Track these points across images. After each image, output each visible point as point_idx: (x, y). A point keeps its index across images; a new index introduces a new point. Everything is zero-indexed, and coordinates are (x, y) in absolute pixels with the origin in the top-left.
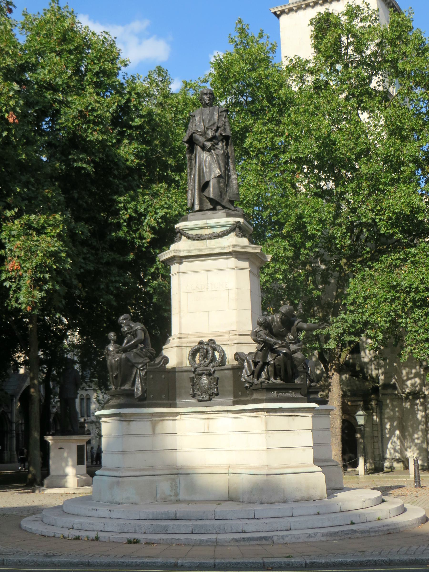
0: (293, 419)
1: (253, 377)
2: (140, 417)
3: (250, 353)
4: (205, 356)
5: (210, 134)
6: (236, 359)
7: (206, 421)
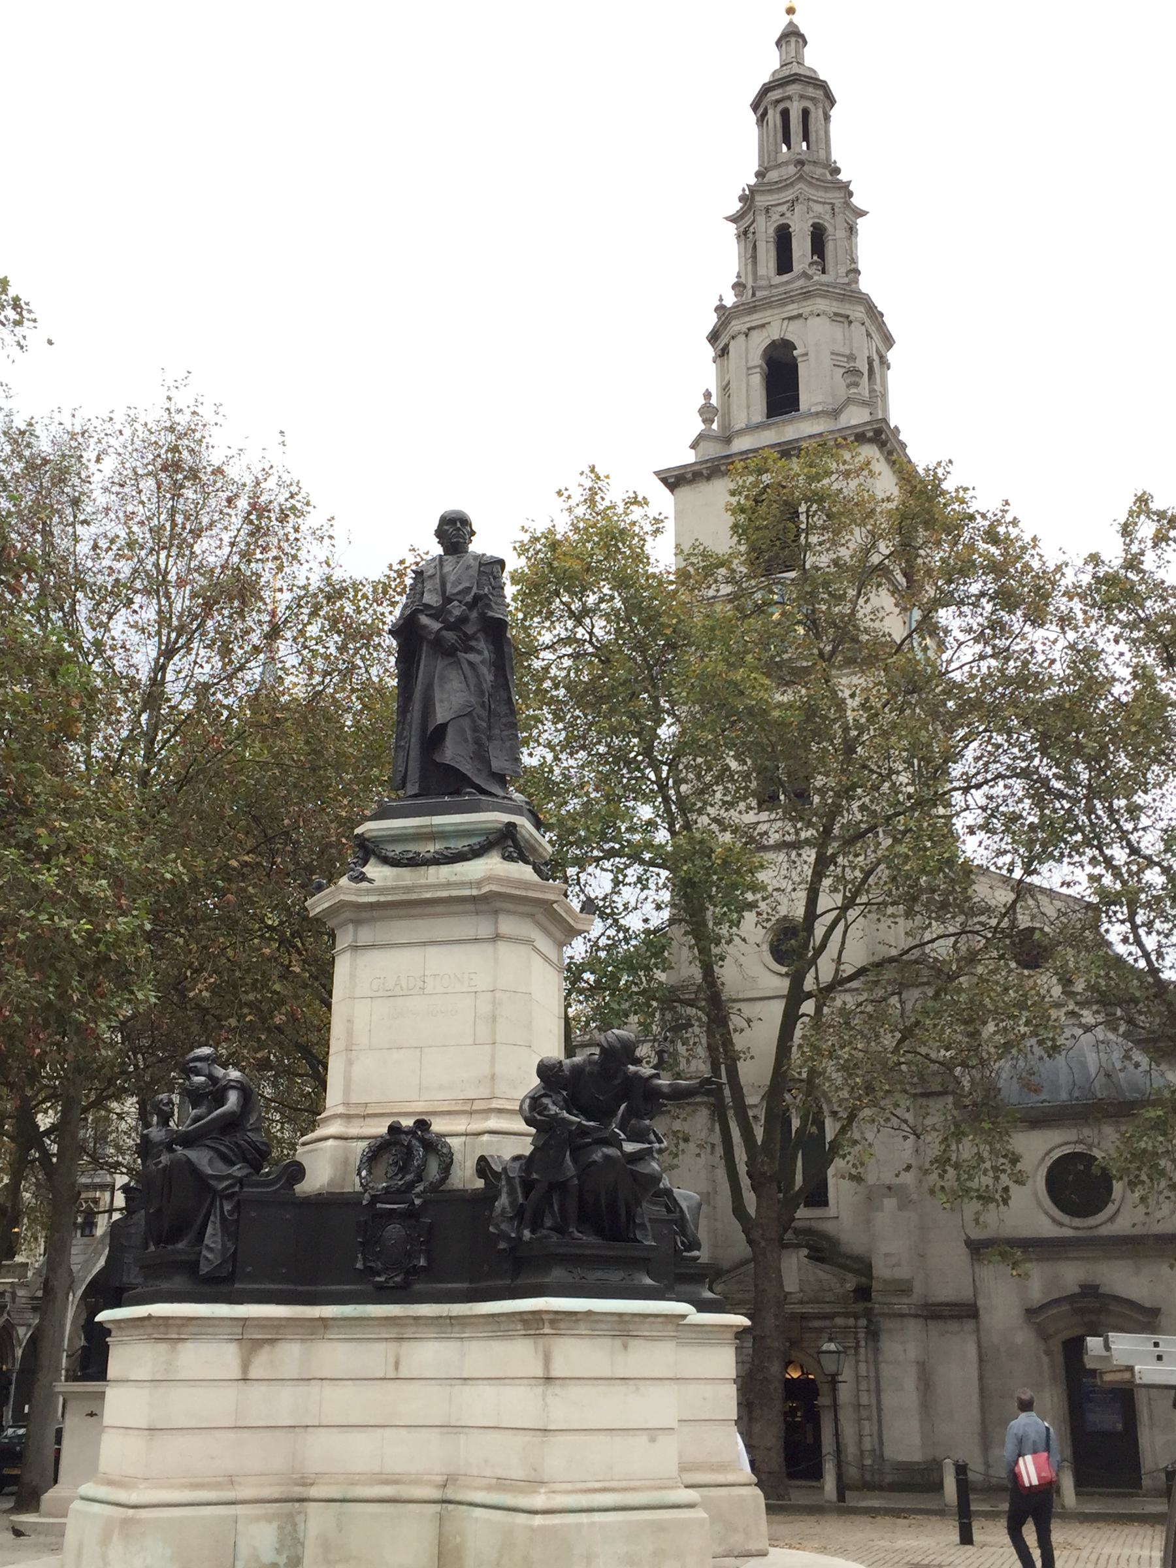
0: (625, 1347)
1: (520, 1224)
2: (210, 1330)
3: (517, 1158)
5: (456, 609)
7: (392, 1346)
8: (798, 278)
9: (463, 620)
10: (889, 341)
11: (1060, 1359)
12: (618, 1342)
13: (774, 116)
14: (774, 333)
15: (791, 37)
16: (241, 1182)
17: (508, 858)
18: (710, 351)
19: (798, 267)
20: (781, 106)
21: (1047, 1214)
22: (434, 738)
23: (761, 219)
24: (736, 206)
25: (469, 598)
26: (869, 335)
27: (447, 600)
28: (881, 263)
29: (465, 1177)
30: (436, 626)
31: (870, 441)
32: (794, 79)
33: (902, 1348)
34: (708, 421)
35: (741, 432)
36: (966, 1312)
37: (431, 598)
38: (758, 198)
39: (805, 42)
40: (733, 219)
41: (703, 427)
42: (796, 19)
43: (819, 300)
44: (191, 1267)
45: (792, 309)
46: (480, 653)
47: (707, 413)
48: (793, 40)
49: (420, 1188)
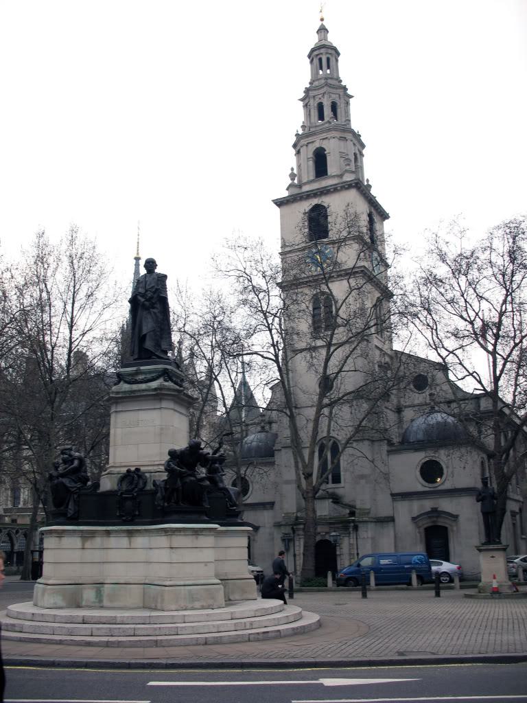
4: (131, 483)
5: (149, 294)
6: (154, 485)
8: (326, 123)
9: (151, 298)
10: (363, 146)
11: (423, 535)
12: (194, 536)
13: (316, 61)
14: (317, 145)
15: (323, 30)
16: (79, 488)
17: (165, 381)
18: (293, 151)
19: (326, 119)
20: (318, 57)
21: (420, 483)
22: (142, 339)
23: (312, 101)
24: (302, 95)
25: (154, 290)
26: (354, 144)
27: (146, 291)
28: (359, 118)
29: (150, 486)
30: (143, 300)
31: (353, 187)
32: (324, 46)
33: (367, 532)
34: (293, 180)
35: (305, 184)
36: (391, 519)
37: (141, 290)
38: (310, 92)
39: (328, 32)
40: (302, 100)
41: (290, 182)
42: (324, 23)
43: (333, 132)
44: (65, 515)
45: (324, 135)
46: (157, 308)
47: (292, 176)
48: (322, 31)
49: (136, 490)
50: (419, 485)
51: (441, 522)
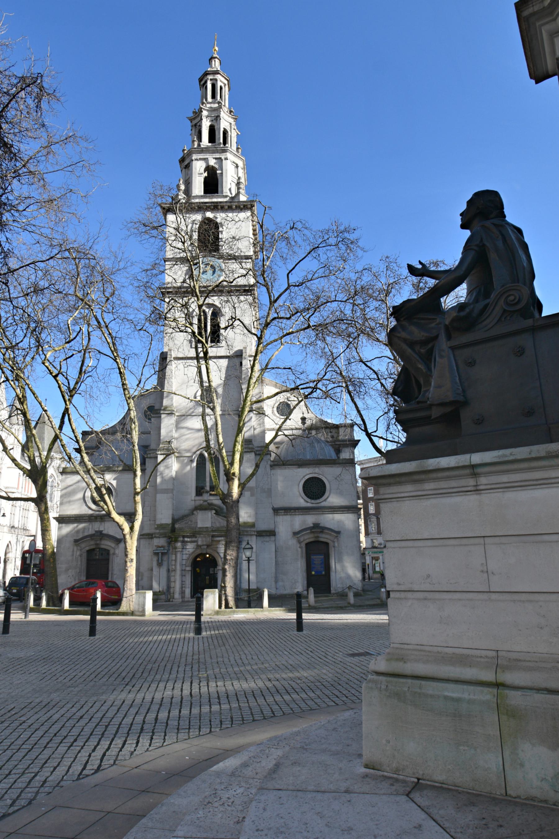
21: (302, 498)
24: (191, 115)
36: (272, 533)
50: (301, 501)
51: (324, 538)
